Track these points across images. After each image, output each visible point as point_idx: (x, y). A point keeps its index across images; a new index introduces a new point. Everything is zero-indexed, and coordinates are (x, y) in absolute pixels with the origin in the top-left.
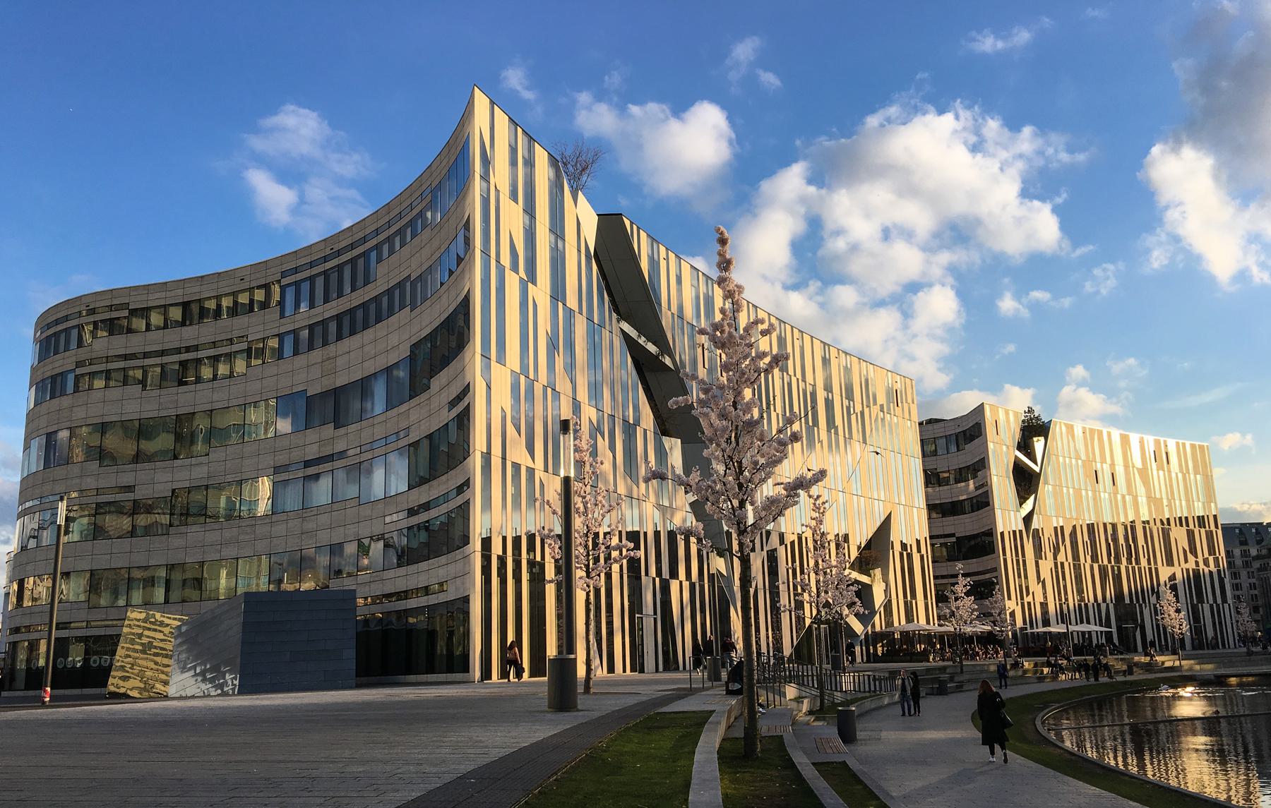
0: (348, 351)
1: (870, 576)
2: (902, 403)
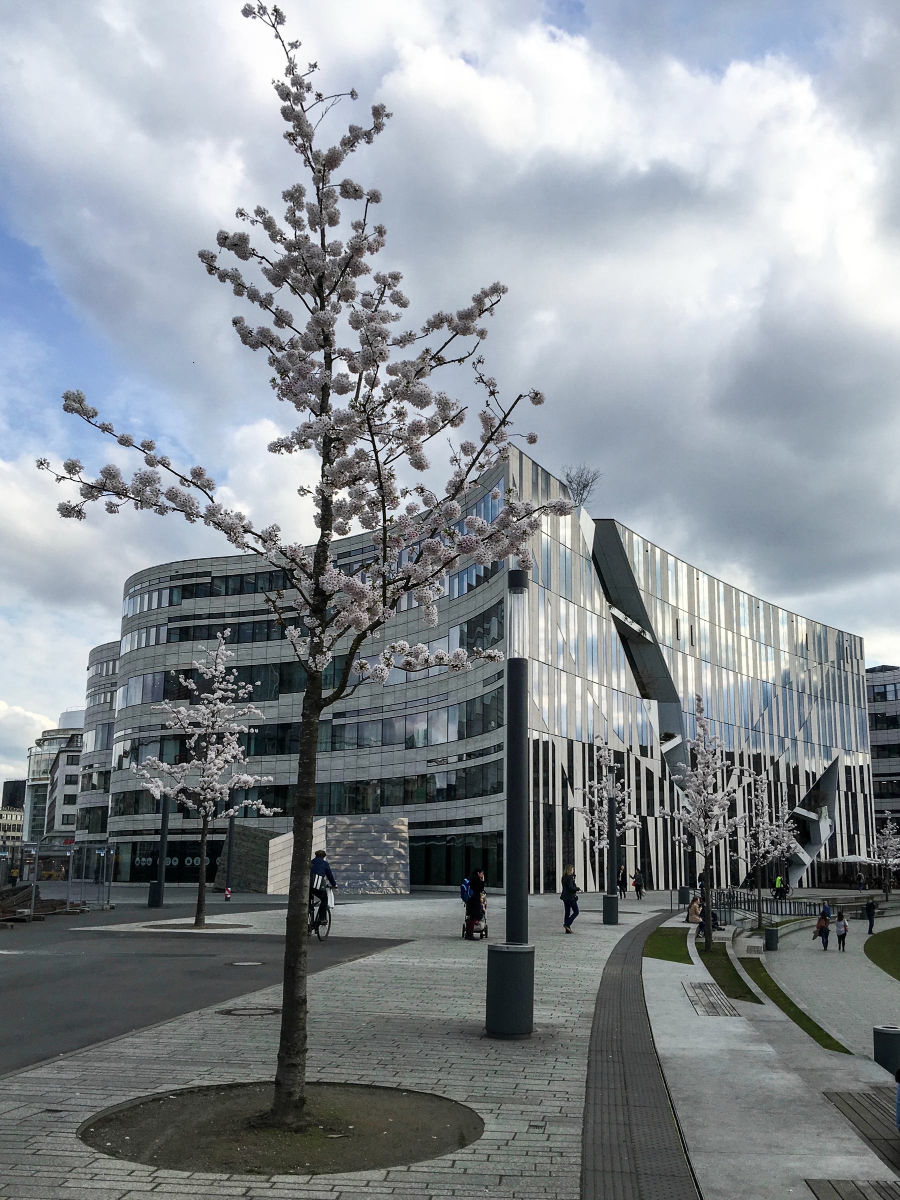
0: (394, 624)
1: (817, 813)
2: (851, 659)
